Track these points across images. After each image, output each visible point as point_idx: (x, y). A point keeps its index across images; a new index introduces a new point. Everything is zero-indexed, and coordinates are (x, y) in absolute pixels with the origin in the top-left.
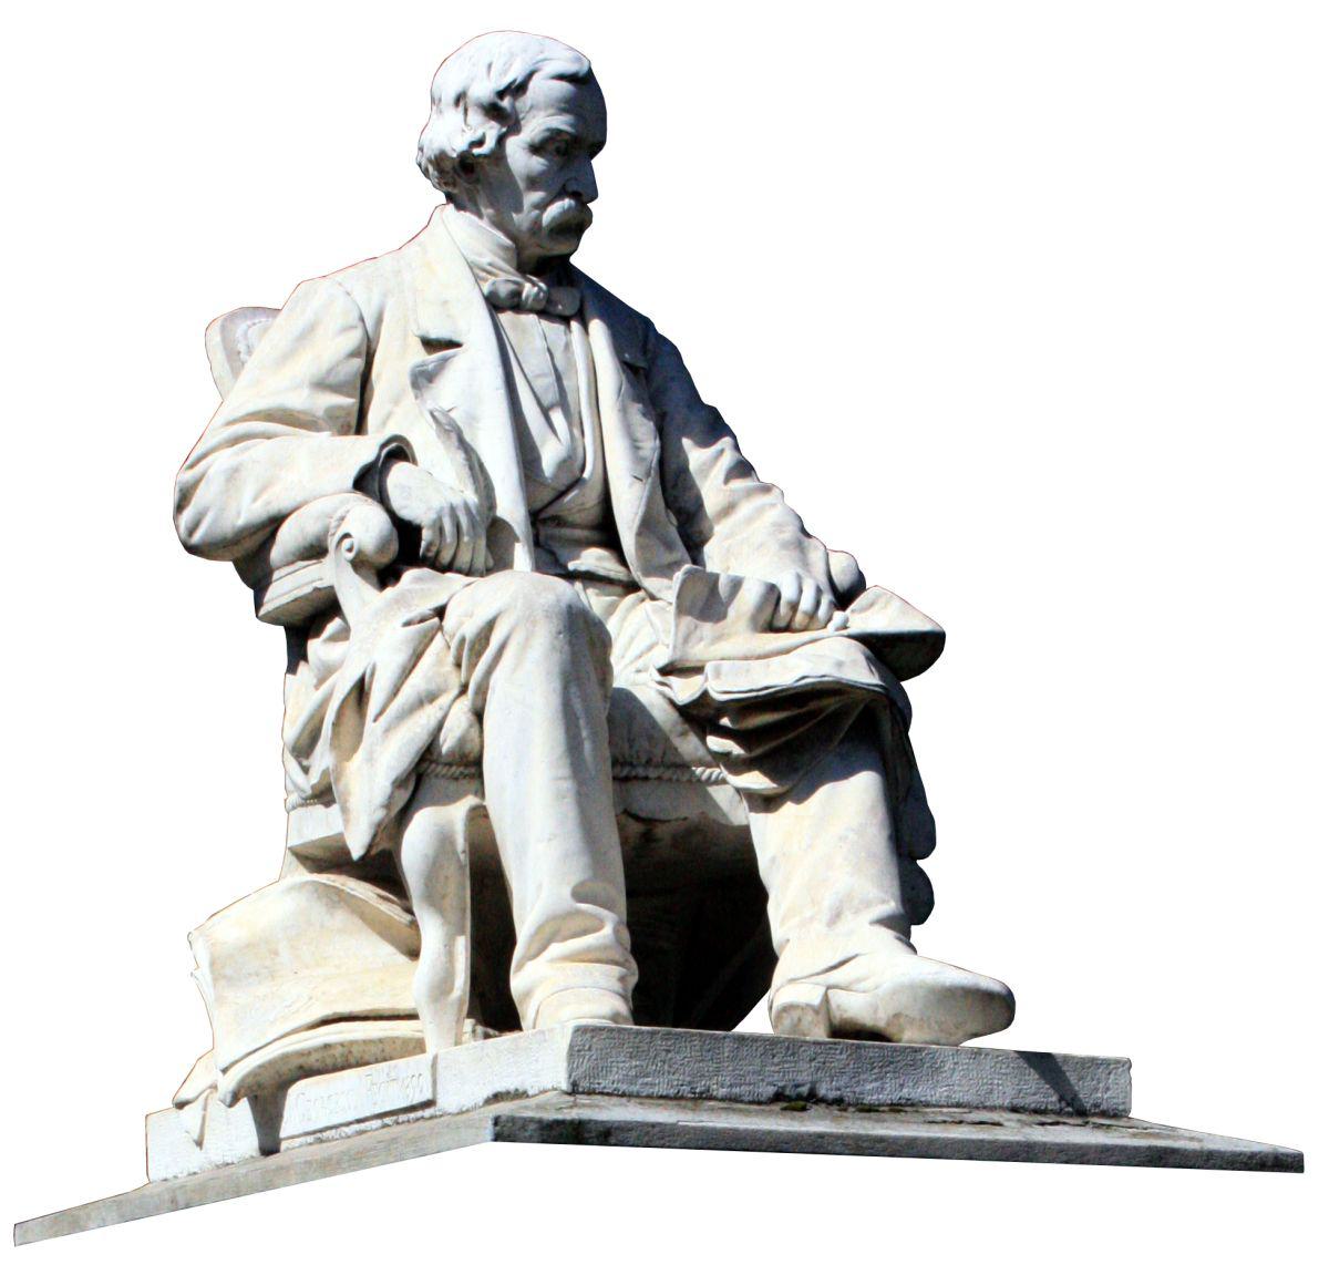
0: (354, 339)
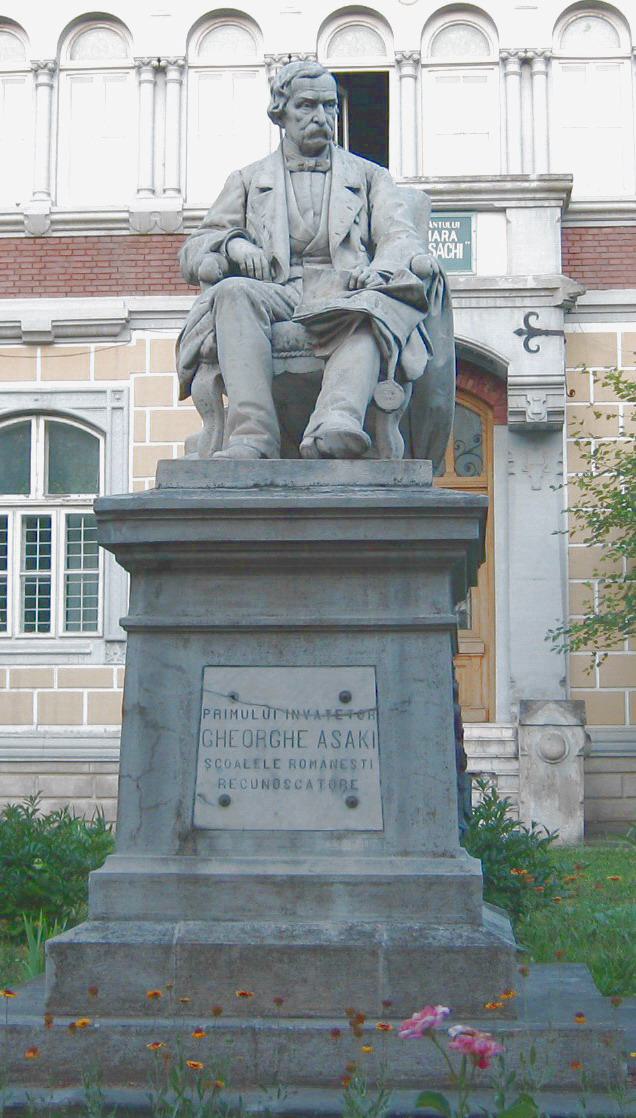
0: (240, 191)
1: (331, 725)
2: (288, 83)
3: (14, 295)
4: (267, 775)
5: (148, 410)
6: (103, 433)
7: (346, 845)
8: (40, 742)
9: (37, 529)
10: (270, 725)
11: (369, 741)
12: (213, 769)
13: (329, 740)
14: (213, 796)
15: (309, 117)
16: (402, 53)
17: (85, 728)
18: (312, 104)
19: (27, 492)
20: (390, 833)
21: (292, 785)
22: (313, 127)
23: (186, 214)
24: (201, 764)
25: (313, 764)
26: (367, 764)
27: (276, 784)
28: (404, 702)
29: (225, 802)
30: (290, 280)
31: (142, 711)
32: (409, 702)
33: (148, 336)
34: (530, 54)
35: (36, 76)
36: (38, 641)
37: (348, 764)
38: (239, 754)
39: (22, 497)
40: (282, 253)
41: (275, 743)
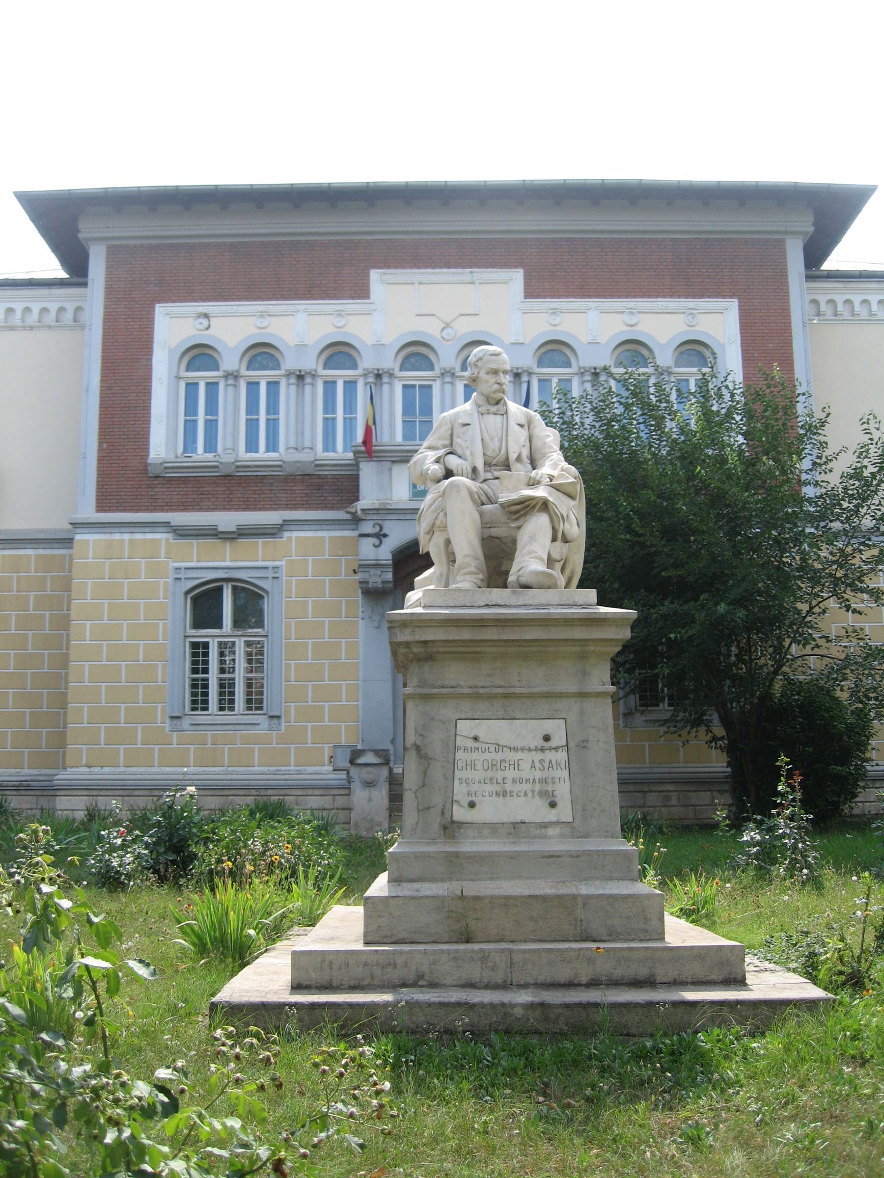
0: (449, 426)
1: (537, 756)
2: (481, 359)
4: (498, 788)
5: (294, 579)
6: (267, 592)
7: (551, 831)
8: (229, 777)
9: (225, 649)
10: (499, 756)
11: (563, 766)
12: (464, 784)
13: (537, 765)
14: (465, 801)
15: (493, 381)
16: (444, 369)
17: (257, 769)
18: (495, 372)
19: (220, 626)
20: (576, 824)
21: (515, 794)
22: (496, 387)
23: (317, 462)
24: (456, 782)
25: (527, 780)
26: (562, 780)
27: (504, 794)
28: (583, 741)
29: (472, 805)
30: (485, 480)
31: (418, 748)
32: (587, 741)
33: (295, 534)
34: (520, 371)
35: (226, 381)
36: (226, 717)
37: (549, 781)
38: (479, 775)
39: (218, 630)
40: (480, 466)
41: (503, 768)
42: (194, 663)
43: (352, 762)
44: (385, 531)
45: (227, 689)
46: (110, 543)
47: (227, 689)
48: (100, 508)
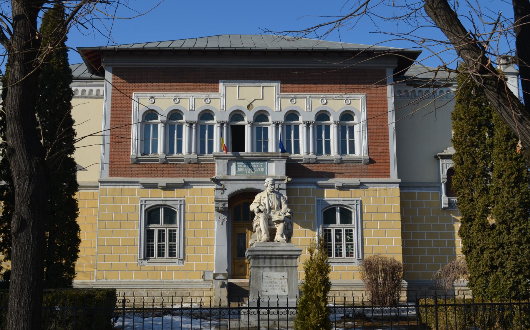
3: (156, 177)
8: (162, 283)
14: (265, 291)
36: (161, 259)
42: (148, 238)
43: (214, 278)
44: (225, 187)
45: (161, 248)
46: (115, 189)
47: (161, 248)
48: (111, 175)
